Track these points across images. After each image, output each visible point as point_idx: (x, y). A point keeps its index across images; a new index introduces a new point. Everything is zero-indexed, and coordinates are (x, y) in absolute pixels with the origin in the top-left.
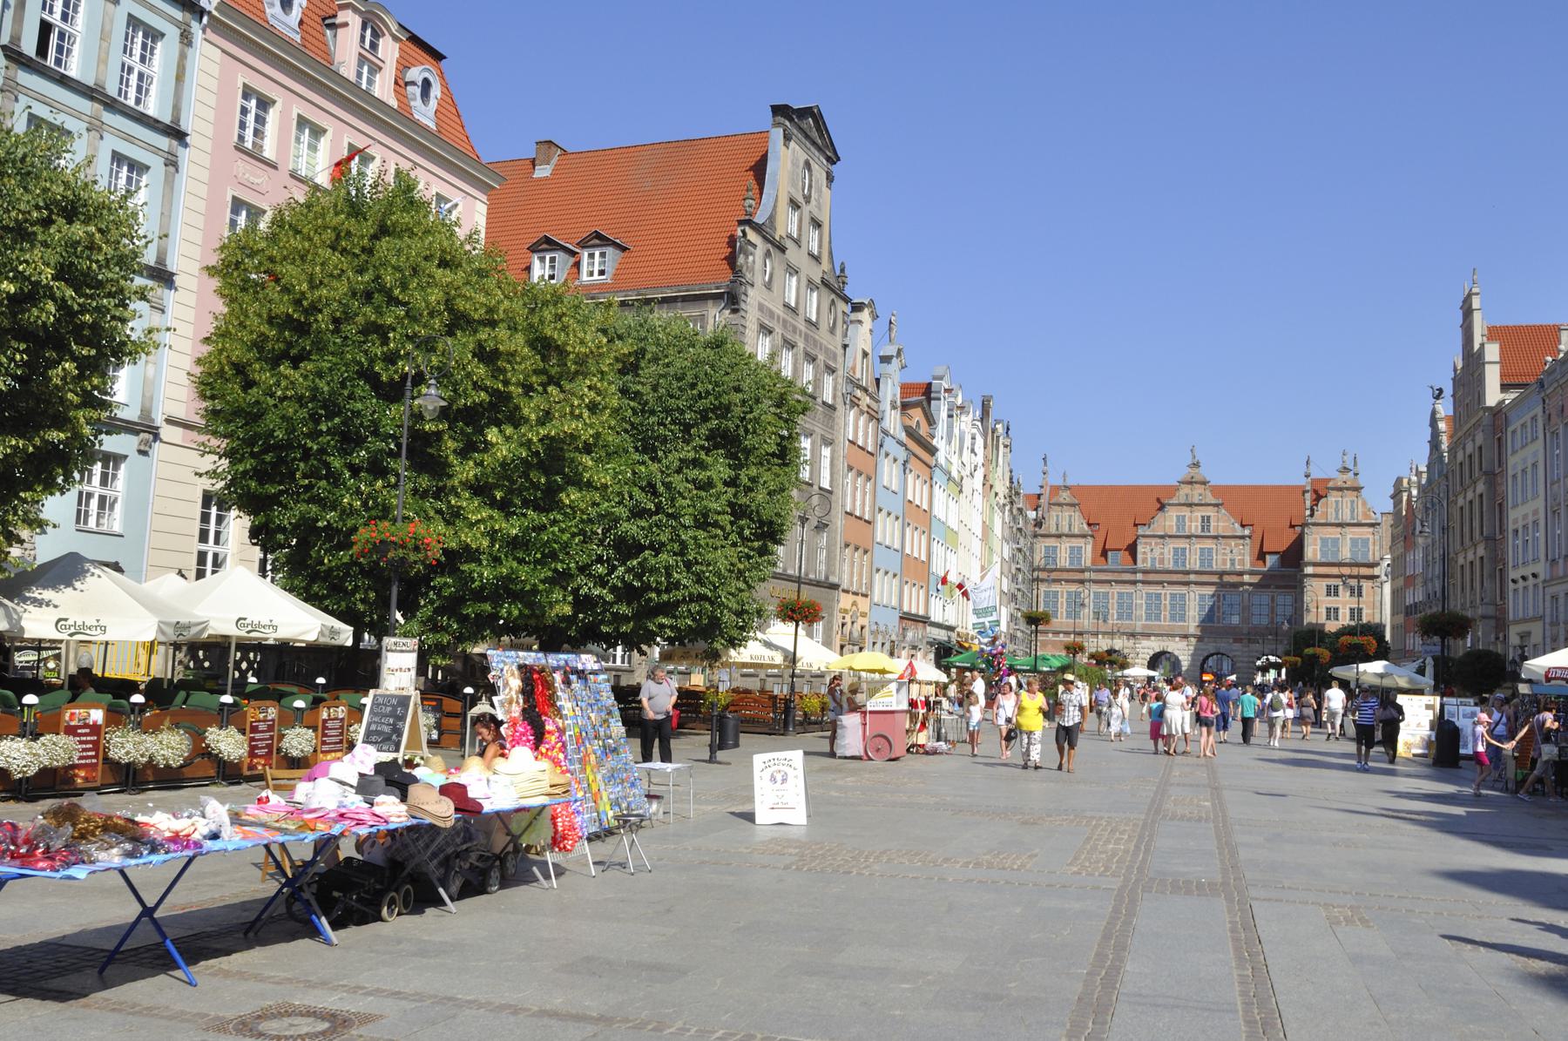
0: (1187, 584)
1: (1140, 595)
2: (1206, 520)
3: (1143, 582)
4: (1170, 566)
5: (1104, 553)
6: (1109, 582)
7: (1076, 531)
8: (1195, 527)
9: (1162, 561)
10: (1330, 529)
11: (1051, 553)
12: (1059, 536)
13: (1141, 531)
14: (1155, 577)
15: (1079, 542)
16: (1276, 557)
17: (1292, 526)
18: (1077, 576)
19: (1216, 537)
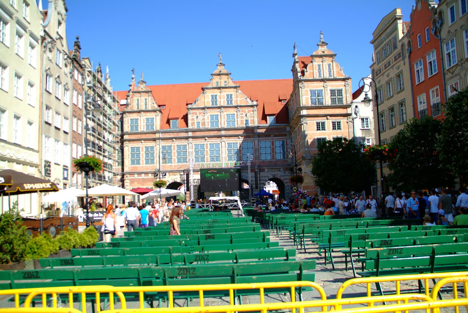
0: (220, 137)
1: (191, 146)
2: (229, 97)
4: (209, 126)
5: (168, 122)
6: (171, 139)
7: (150, 108)
8: (222, 101)
9: (204, 124)
10: (316, 84)
11: (135, 123)
12: (139, 112)
13: (189, 106)
16: (273, 118)
17: (280, 100)
19: (236, 107)
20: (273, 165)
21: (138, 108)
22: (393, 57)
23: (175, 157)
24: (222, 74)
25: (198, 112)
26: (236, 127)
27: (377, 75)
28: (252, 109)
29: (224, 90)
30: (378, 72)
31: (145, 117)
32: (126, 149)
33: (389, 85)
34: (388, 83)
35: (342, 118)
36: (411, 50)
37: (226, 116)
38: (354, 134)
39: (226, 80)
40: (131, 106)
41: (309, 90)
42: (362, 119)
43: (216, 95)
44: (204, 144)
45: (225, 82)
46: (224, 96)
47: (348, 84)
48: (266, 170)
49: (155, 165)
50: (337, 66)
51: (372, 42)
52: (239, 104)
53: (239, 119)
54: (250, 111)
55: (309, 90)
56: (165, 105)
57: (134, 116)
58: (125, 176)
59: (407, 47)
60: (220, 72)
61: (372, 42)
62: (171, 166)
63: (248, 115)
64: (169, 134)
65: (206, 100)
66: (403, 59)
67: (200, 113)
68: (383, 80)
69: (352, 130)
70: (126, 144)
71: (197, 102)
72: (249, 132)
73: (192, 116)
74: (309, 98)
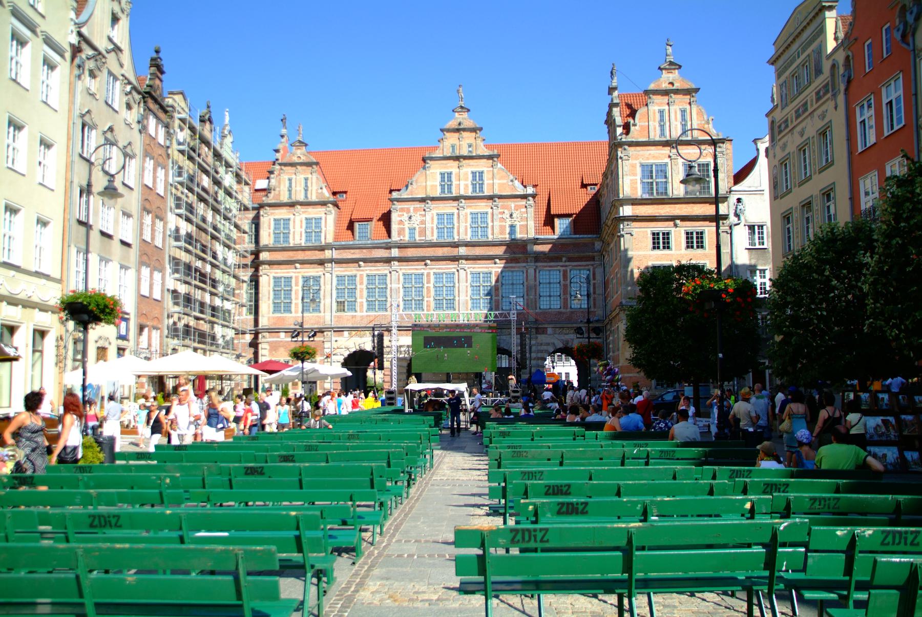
0: (455, 259)
2: (478, 177)
3: (400, 260)
4: (433, 237)
5: (351, 227)
6: (355, 261)
7: (313, 198)
8: (463, 186)
9: (423, 232)
11: (282, 226)
12: (292, 205)
13: (395, 195)
14: (416, 253)
15: (314, 212)
16: (567, 222)
17: (584, 186)
18: (315, 255)
19: (491, 198)
20: (561, 319)
21: (290, 197)
22: (814, 93)
23: (362, 298)
24: (464, 130)
25: (411, 206)
26: (490, 239)
27: (780, 132)
28: (523, 202)
29: (467, 161)
30: (783, 126)
31: (304, 216)
32: (263, 281)
33: (804, 154)
34: (802, 149)
35: (707, 223)
36: (849, 77)
37: (469, 217)
38: (732, 258)
39: (472, 141)
40: (277, 192)
41: (638, 165)
42: (751, 228)
43: (451, 173)
44: (422, 274)
45: (470, 146)
46: (466, 174)
47: (722, 152)
48: (550, 331)
49: (322, 314)
50: (699, 113)
51: (773, 62)
52: (497, 192)
53: (497, 223)
54: (520, 207)
55: (637, 163)
56: (345, 192)
57: (281, 214)
58: (260, 336)
59: (841, 70)
60: (460, 124)
61: (773, 62)
62: (353, 317)
63: (514, 216)
64: (352, 251)
65: (428, 183)
66: (834, 96)
67: (416, 210)
68: (793, 142)
69: (729, 251)
70: (263, 269)
71: (410, 187)
72: (517, 251)
73: (399, 216)
74: (639, 181)
